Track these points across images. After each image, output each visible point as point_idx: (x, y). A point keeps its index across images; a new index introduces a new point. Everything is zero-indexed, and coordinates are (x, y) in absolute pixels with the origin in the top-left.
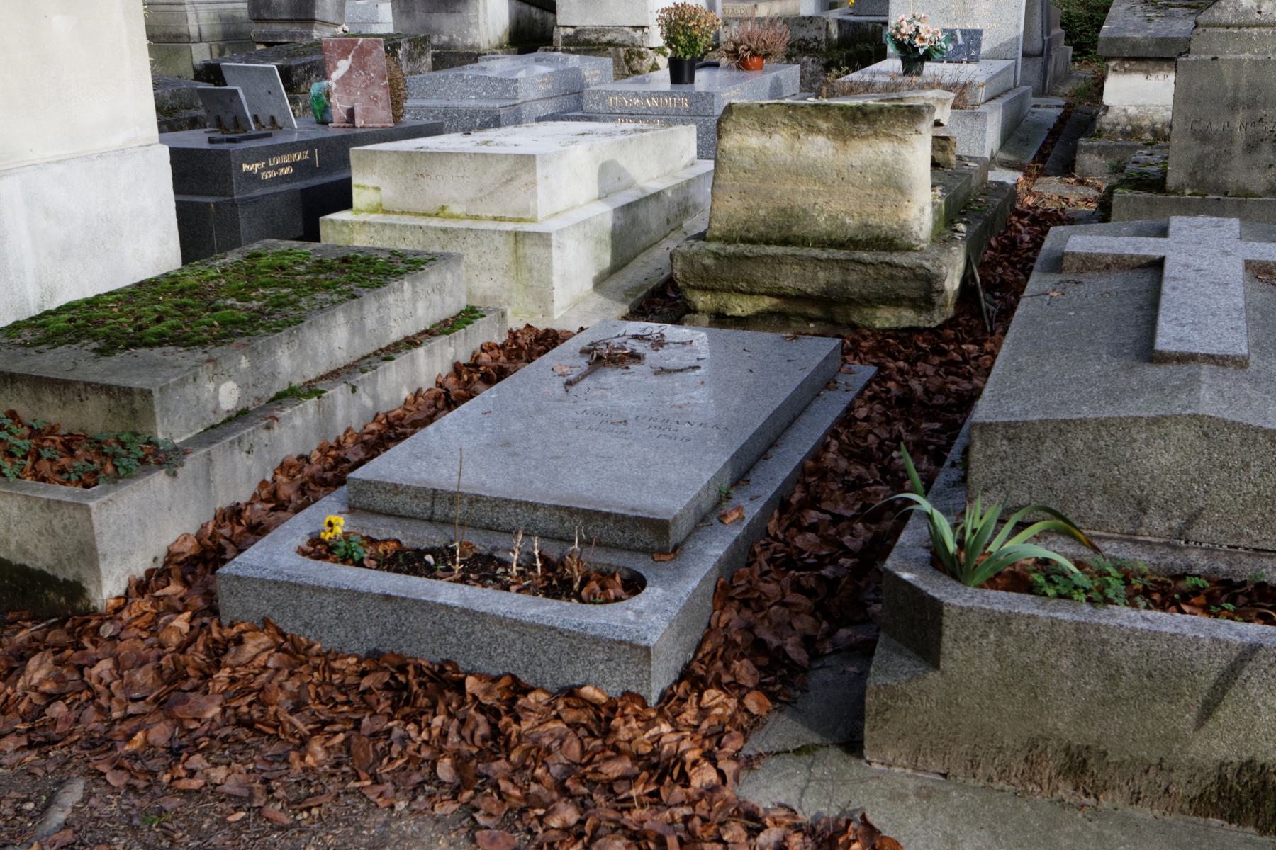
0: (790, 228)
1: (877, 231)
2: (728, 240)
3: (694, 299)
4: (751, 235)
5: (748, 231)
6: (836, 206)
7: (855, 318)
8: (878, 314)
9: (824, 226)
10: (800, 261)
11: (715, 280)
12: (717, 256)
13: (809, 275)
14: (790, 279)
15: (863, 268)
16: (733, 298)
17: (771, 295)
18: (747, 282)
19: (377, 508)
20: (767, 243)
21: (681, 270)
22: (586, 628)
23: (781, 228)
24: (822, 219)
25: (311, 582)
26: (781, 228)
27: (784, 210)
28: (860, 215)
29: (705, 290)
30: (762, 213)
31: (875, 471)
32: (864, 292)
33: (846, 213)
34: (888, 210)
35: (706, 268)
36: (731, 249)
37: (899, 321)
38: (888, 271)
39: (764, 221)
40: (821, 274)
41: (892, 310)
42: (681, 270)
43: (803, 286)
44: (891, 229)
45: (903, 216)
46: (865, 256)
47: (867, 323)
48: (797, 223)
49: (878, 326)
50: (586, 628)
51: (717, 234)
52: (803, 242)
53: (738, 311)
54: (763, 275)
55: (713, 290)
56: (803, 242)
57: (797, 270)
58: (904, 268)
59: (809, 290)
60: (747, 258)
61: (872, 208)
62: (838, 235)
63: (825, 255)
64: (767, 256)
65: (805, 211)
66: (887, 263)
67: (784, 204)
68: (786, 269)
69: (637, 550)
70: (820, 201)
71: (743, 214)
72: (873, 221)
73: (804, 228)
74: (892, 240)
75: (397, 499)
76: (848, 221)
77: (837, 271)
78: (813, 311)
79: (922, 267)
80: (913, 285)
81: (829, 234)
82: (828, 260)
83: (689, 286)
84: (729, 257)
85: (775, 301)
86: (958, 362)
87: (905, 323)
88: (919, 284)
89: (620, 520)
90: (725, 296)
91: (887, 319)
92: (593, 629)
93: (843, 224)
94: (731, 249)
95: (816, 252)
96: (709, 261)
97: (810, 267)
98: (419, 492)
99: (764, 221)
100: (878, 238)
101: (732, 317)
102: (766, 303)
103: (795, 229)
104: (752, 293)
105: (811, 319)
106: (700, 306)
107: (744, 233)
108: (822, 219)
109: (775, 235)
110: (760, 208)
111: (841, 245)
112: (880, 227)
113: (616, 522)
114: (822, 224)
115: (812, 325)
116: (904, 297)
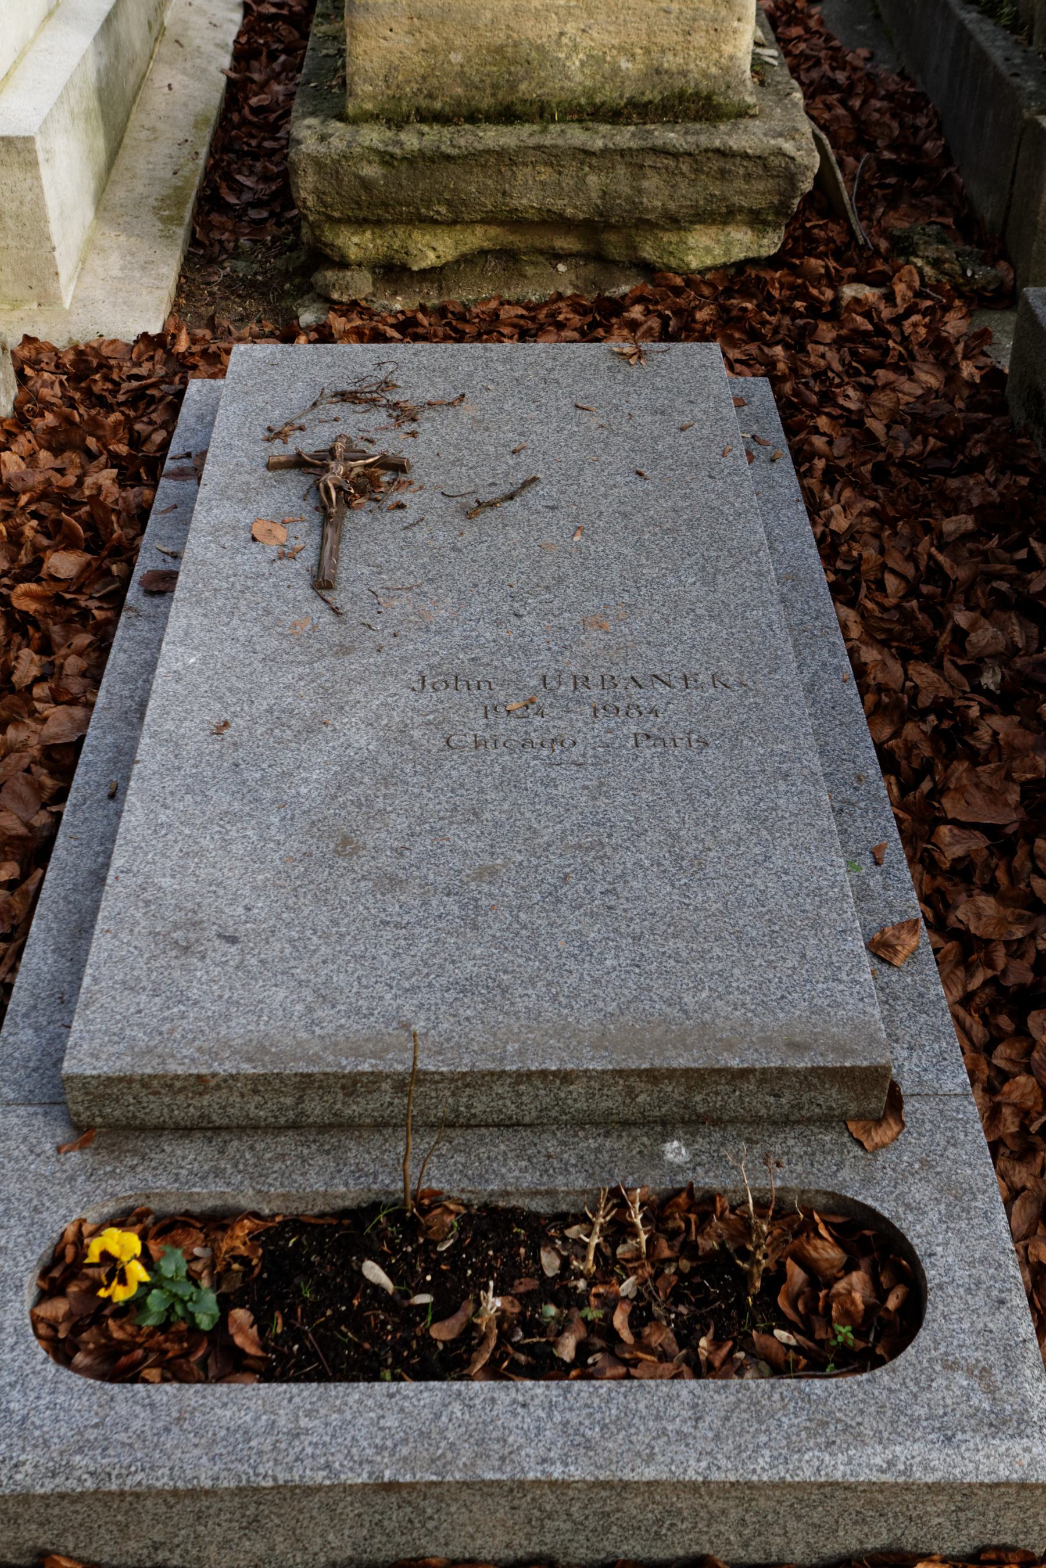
0: (513, 86)
1: (679, 82)
2: (396, 121)
3: (339, 242)
4: (438, 105)
5: (430, 96)
6: (602, 37)
7: (648, 252)
8: (691, 242)
9: (579, 77)
10: (552, 157)
11: (385, 204)
12: (386, 159)
13: (568, 182)
14: (530, 191)
15: (671, 163)
16: (416, 235)
17: (488, 220)
18: (449, 203)
19: (151, 1121)
20: (472, 118)
21: (316, 191)
22: (908, 1470)
23: (495, 86)
24: (574, 64)
25: (162, 1481)
26: (495, 86)
27: (500, 50)
28: (647, 51)
29: (360, 223)
30: (456, 58)
31: (955, 674)
32: (672, 206)
33: (621, 49)
34: (699, 39)
35: (366, 184)
36: (410, 140)
37: (727, 252)
38: (716, 164)
39: (462, 74)
40: (592, 179)
41: (713, 231)
42: (316, 191)
43: (558, 204)
44: (705, 75)
45: (727, 49)
46: (671, 136)
47: (674, 263)
48: (528, 76)
49: (694, 264)
50: (908, 1470)
51: (369, 106)
52: (541, 112)
53: (430, 259)
54: (475, 186)
55: (379, 223)
56: (541, 112)
57: (546, 174)
58: (746, 156)
59: (569, 211)
60: (448, 158)
61: (669, 38)
62: (609, 94)
63: (599, 144)
64: (488, 152)
65: (540, 49)
66: (718, 151)
67: (500, 38)
68: (523, 173)
69: (810, 1121)
70: (571, 28)
71: (418, 63)
72: (670, 62)
73: (541, 85)
74: (709, 98)
75: (206, 1100)
76: (624, 64)
77: (621, 171)
78: (564, 243)
79: (780, 153)
80: (761, 186)
81: (590, 93)
82: (605, 151)
83: (330, 219)
84: (411, 160)
85: (493, 231)
86: (865, 333)
87: (738, 254)
88: (771, 183)
89: (771, 1079)
90: (400, 231)
91: (708, 250)
92: (927, 1468)
93: (616, 70)
94: (410, 140)
95: (576, 136)
96: (371, 171)
97: (571, 168)
98: (259, 1084)
99: (462, 74)
100: (681, 96)
101: (423, 272)
102: (476, 238)
103: (523, 87)
104: (453, 223)
105: (556, 256)
106: (353, 253)
107: (424, 103)
108: (574, 64)
109: (486, 102)
110: (451, 49)
111: (614, 116)
112: (684, 74)
113: (761, 1082)
114: (575, 75)
115: (561, 268)
116: (741, 209)
